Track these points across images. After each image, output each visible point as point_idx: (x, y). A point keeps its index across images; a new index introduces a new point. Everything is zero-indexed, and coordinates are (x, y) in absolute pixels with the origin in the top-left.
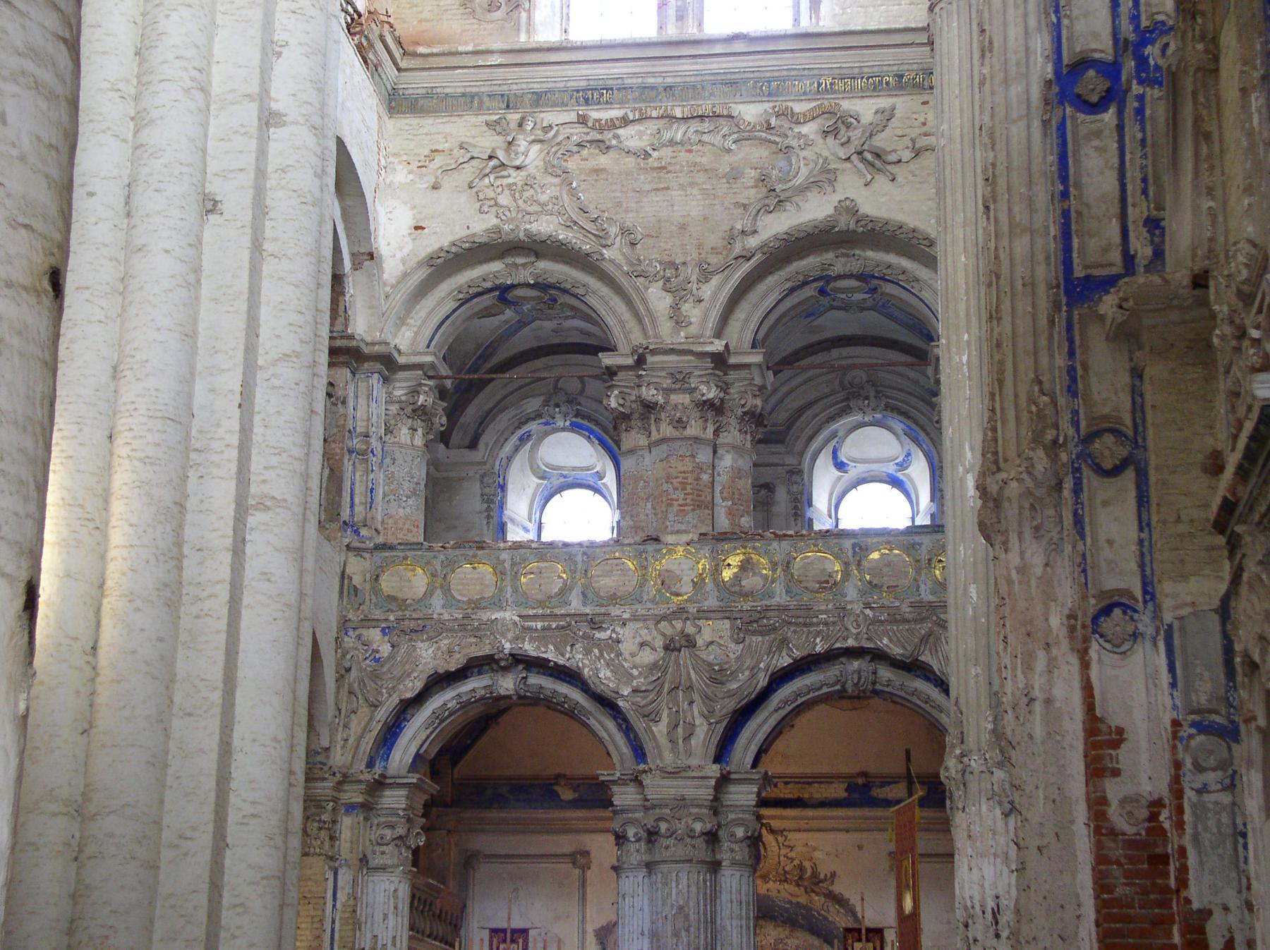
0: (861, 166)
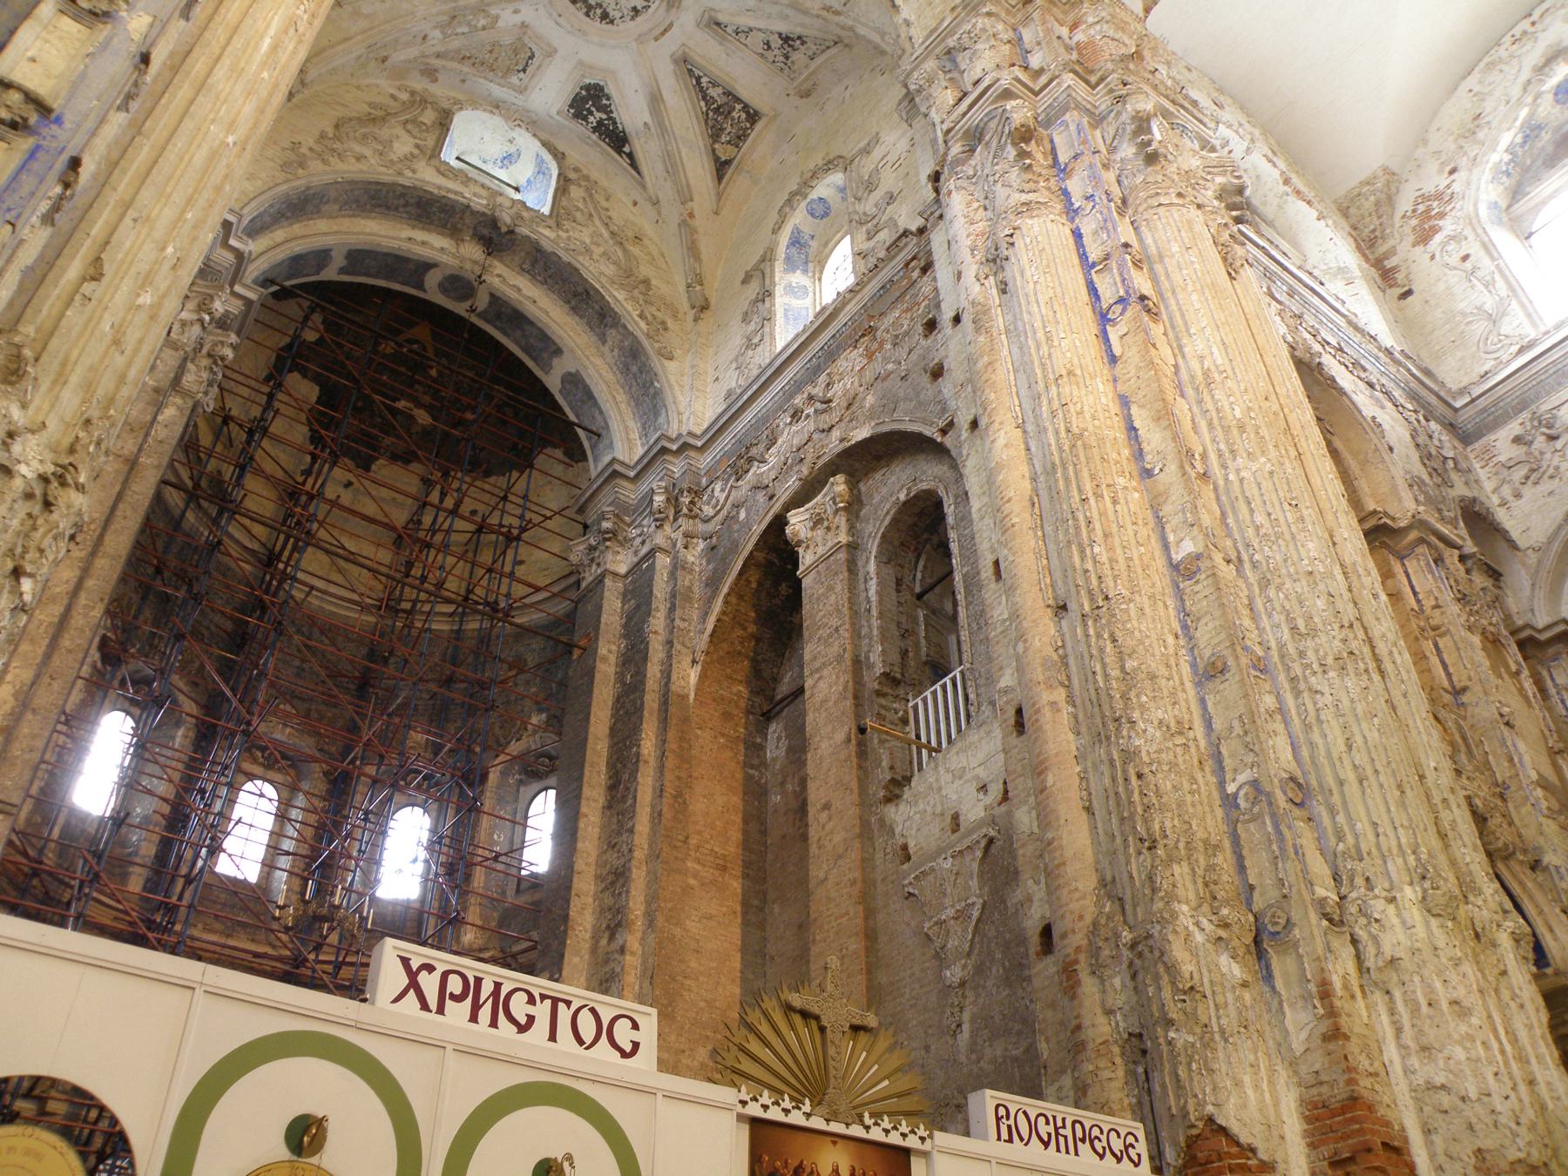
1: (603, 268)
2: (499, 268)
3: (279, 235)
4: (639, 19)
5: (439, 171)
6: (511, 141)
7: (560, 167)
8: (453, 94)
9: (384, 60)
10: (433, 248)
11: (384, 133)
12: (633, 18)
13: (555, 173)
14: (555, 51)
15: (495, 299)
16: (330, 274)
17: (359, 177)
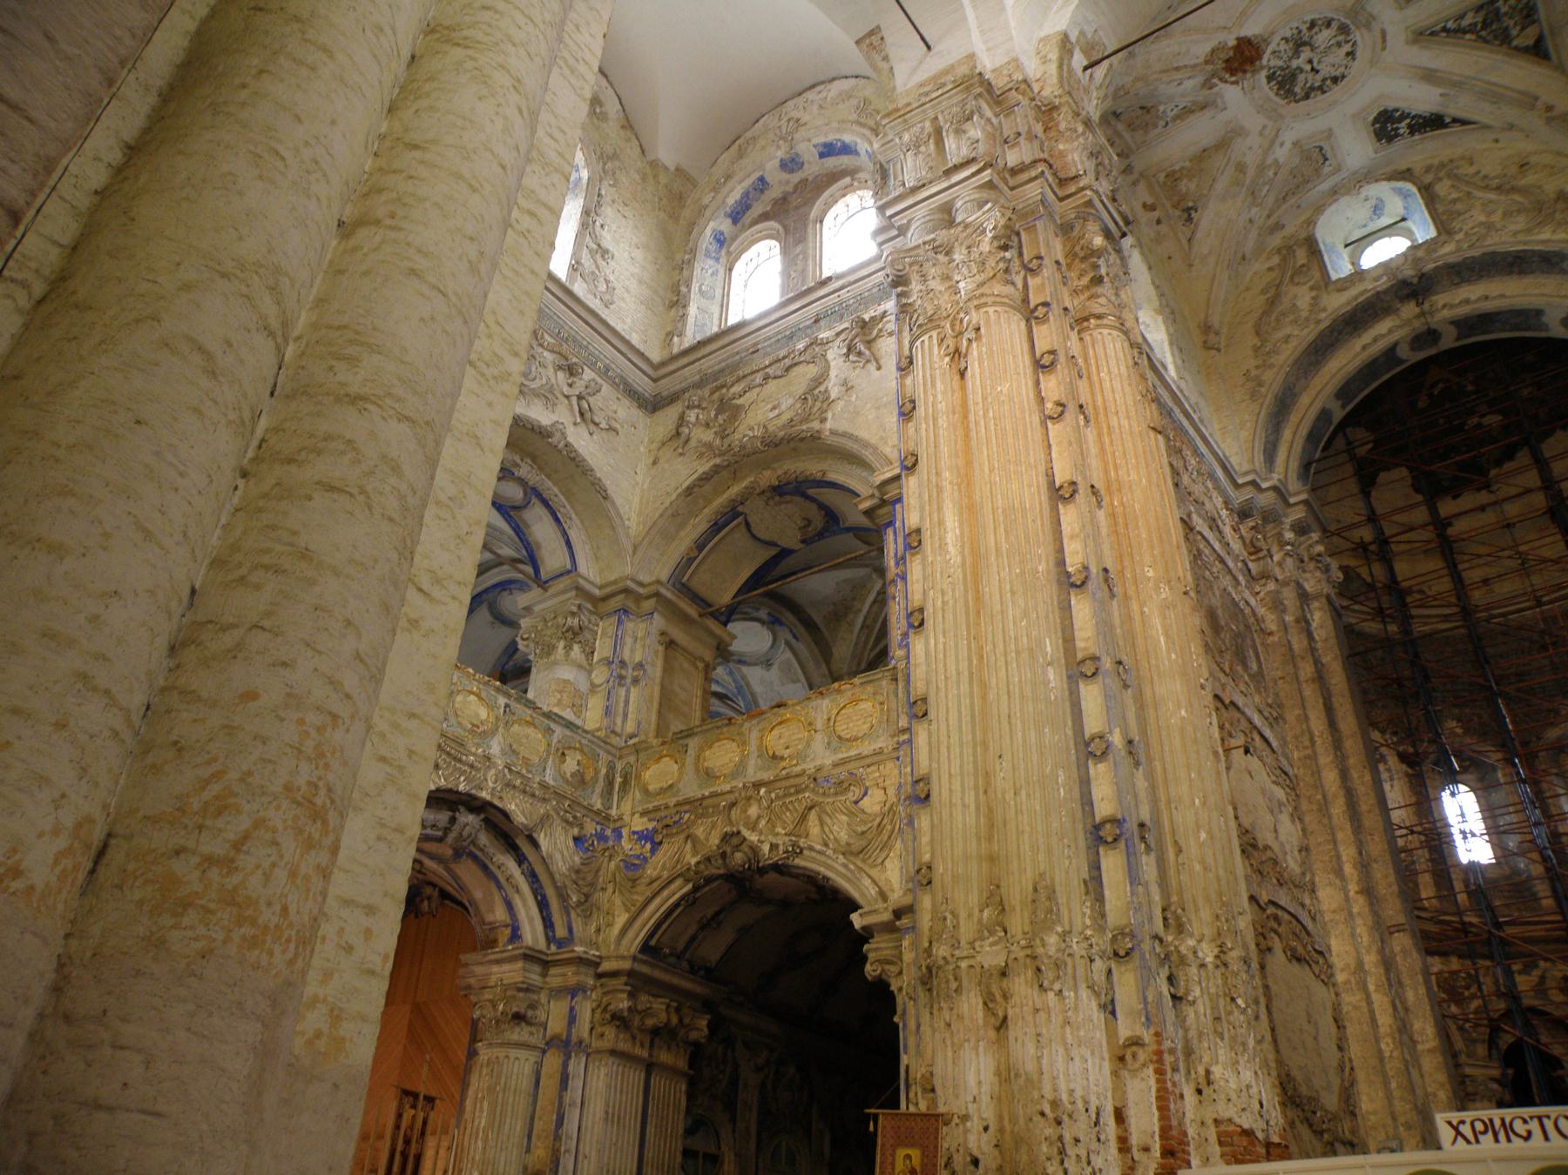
0: (576, 408)
1: (1512, 227)
2: (1440, 299)
3: (1287, 434)
4: (1358, 54)
5: (1339, 290)
6: (1366, 200)
7: (1415, 184)
8: (1303, 218)
9: (1244, 258)
10: (1383, 336)
11: (1285, 303)
12: (1354, 59)
13: (1414, 190)
14: (1331, 130)
15: (1456, 323)
16: (1338, 414)
17: (1297, 354)
